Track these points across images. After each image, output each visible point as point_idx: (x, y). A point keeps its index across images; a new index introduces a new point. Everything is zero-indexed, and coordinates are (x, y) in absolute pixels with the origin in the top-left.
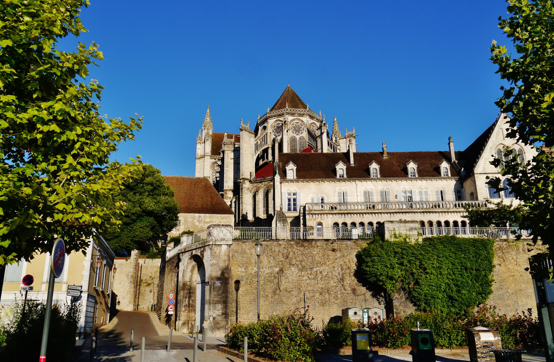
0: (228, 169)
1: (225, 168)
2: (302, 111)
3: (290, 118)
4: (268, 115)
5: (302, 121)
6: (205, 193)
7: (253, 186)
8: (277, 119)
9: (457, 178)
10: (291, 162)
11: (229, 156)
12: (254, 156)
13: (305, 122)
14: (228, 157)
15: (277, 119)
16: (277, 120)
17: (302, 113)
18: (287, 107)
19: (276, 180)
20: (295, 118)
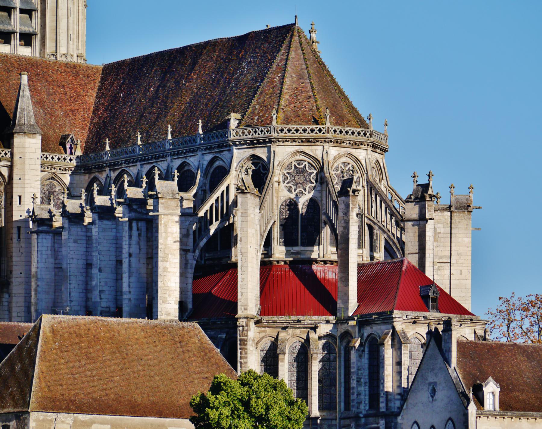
0: (167, 264)
1: (160, 264)
2: (359, 133)
3: (333, 151)
4: (274, 134)
5: (357, 160)
6: (208, 368)
7: (264, 334)
8: (297, 148)
10: (490, 378)
11: (169, 230)
12: (259, 253)
13: (363, 163)
14: (166, 232)
15: (297, 148)
16: (297, 152)
17: (359, 139)
18: (328, 124)
19: (470, 411)
20: (343, 150)
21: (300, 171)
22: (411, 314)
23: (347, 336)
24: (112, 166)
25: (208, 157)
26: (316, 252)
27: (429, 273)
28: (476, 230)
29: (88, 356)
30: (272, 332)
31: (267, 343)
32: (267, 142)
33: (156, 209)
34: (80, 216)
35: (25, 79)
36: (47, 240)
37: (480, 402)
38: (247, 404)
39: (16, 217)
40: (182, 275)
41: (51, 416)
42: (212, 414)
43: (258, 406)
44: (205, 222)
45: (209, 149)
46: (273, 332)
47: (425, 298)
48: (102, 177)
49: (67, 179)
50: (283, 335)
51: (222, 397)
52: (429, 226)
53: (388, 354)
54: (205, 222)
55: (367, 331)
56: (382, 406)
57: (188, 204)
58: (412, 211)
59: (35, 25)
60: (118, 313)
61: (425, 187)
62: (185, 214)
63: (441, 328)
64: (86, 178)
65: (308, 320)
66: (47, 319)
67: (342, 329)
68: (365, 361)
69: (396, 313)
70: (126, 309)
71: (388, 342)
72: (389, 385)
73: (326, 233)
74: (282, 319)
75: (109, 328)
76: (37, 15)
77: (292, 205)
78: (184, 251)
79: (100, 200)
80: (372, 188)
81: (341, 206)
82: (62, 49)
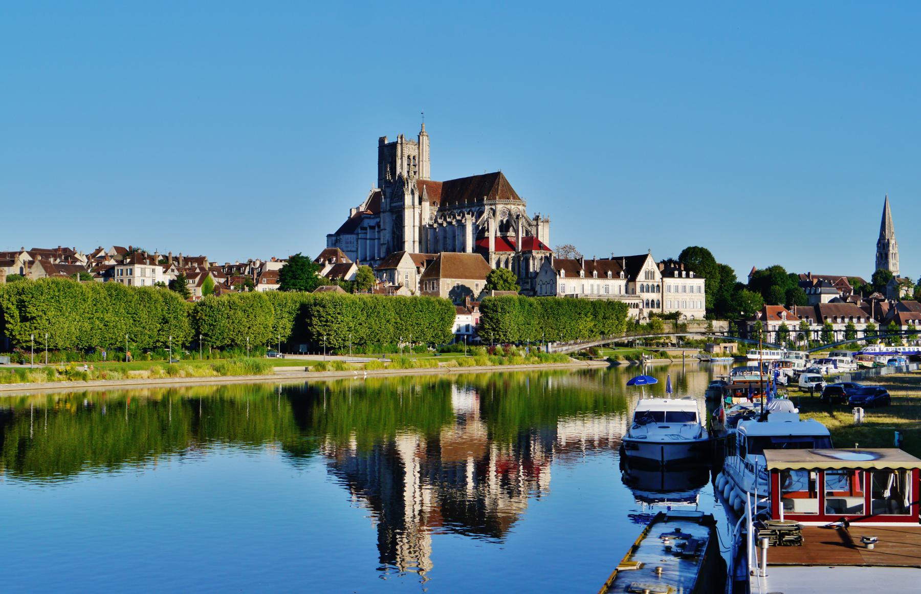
3: (513, 207)
9: (627, 279)
21: (504, 212)
22: (537, 251)
23: (519, 257)
24: (449, 210)
25: (478, 208)
26: (508, 234)
27: (539, 239)
28: (550, 227)
29: (454, 263)
30: (499, 256)
31: (497, 259)
32: (495, 204)
33: (465, 222)
34: (442, 224)
35: (425, 186)
36: (432, 230)
37: (560, 275)
38: (501, 276)
39: (423, 224)
40: (473, 240)
41: (445, 279)
42: (493, 279)
43: (505, 277)
44: (478, 226)
45: (478, 206)
46: (499, 256)
47: (540, 247)
48: (446, 213)
49: (435, 213)
50: (501, 257)
51: (495, 275)
52: (539, 227)
53: (531, 262)
54: (478, 226)
55: (525, 256)
56: (529, 276)
57: (474, 221)
58: (535, 223)
59: (417, 169)
60: (454, 251)
61: (538, 216)
62: (473, 224)
63: (548, 255)
64: (441, 213)
65: (508, 252)
66: (443, 253)
67: (517, 255)
68: (524, 264)
69: (533, 251)
70: (457, 249)
71: (531, 258)
72: (531, 270)
73: (511, 229)
74: (501, 252)
75: (458, 255)
76: (417, 167)
77: (502, 221)
78: (473, 234)
79: (449, 220)
80: (523, 216)
81: (517, 222)
82: (424, 176)
